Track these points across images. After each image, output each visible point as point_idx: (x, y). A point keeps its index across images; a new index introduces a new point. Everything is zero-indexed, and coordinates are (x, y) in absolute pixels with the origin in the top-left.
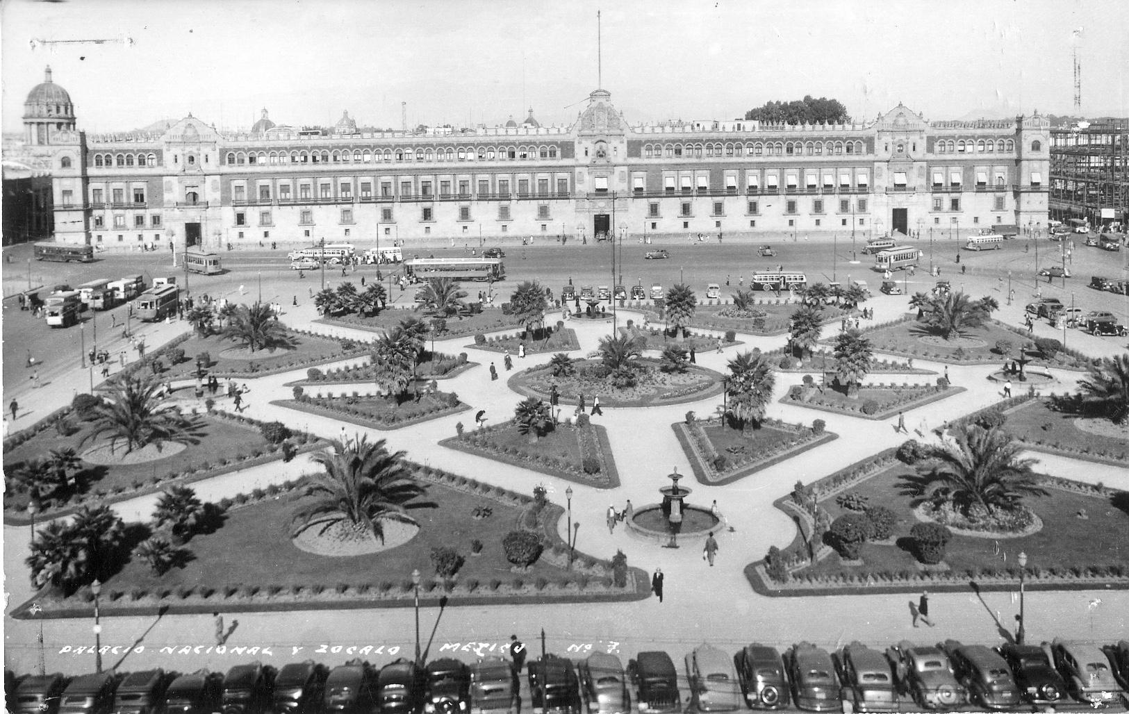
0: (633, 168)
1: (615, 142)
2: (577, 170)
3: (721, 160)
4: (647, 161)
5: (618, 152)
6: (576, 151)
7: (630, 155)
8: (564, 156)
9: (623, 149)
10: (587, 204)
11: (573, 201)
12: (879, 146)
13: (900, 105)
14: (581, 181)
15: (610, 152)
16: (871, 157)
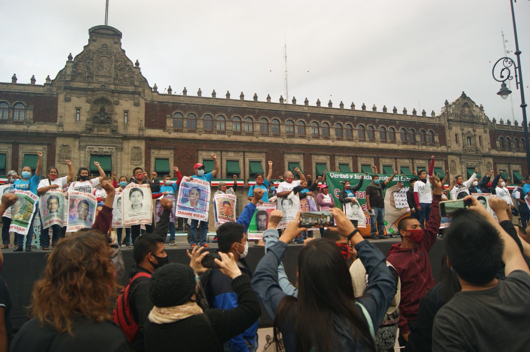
0: (152, 143)
1: (126, 104)
2: (60, 142)
3: (280, 140)
6: (60, 110)
7: (150, 124)
8: (38, 118)
9: (138, 114)
12: (450, 135)
13: (464, 96)
15: (119, 118)
16: (443, 149)
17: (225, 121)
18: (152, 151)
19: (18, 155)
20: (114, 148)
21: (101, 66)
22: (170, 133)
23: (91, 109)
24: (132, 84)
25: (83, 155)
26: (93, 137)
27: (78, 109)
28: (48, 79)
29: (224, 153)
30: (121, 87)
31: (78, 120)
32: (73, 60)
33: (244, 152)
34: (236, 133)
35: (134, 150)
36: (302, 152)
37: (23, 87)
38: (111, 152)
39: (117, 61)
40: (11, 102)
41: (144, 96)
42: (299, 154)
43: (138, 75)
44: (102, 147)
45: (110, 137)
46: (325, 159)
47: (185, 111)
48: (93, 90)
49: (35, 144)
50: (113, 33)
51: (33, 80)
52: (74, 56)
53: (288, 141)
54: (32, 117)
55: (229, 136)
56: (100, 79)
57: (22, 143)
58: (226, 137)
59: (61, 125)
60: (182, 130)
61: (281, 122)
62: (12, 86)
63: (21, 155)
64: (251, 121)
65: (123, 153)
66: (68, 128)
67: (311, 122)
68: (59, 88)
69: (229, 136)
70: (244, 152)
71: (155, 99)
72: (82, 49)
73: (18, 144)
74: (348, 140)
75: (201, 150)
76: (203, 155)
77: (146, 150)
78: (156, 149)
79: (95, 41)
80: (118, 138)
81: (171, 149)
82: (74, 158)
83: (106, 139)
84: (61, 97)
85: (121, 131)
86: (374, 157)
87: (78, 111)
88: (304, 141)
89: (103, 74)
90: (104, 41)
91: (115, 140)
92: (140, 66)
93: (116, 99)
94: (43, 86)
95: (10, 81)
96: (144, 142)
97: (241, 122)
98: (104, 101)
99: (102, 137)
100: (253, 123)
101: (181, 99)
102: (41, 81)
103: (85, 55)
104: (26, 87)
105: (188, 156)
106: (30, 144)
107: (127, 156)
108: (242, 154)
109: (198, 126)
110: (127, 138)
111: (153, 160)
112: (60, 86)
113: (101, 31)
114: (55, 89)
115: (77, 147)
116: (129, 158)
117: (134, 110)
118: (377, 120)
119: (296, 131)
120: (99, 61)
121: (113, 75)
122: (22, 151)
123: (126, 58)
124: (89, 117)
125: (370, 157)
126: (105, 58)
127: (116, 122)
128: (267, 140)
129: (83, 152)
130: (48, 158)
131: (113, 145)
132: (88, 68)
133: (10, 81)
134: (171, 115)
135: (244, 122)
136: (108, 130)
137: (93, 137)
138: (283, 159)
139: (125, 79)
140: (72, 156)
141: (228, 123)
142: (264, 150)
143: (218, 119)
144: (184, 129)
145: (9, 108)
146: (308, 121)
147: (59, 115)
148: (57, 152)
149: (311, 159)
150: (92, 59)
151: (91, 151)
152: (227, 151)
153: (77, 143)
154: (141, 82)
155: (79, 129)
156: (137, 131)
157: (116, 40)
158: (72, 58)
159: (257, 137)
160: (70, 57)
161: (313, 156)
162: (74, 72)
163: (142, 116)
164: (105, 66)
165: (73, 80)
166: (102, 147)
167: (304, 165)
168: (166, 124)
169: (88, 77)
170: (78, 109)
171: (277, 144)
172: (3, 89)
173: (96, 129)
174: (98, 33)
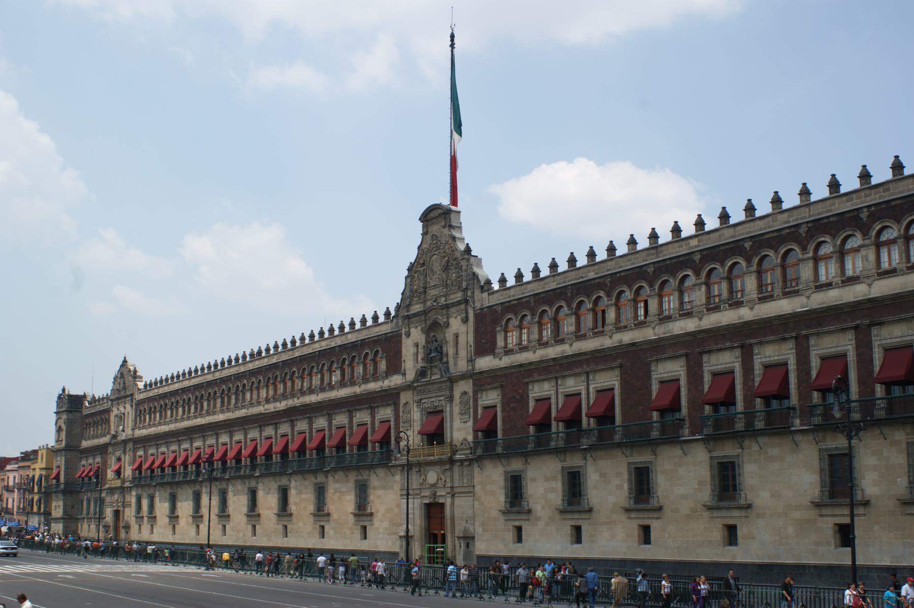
0: (482, 381)
20: (442, 398)
46: (733, 359)
55: (571, 345)
59: (404, 374)
69: (571, 345)
70: (587, 373)
74: (786, 294)
86: (856, 328)
88: (690, 325)
96: (471, 381)
108: (584, 378)
111: (480, 411)
113: (434, 214)
117: (463, 328)
118: (864, 215)
125: (843, 330)
142: (617, 363)
149: (700, 365)
167: (689, 382)
170: (417, 345)
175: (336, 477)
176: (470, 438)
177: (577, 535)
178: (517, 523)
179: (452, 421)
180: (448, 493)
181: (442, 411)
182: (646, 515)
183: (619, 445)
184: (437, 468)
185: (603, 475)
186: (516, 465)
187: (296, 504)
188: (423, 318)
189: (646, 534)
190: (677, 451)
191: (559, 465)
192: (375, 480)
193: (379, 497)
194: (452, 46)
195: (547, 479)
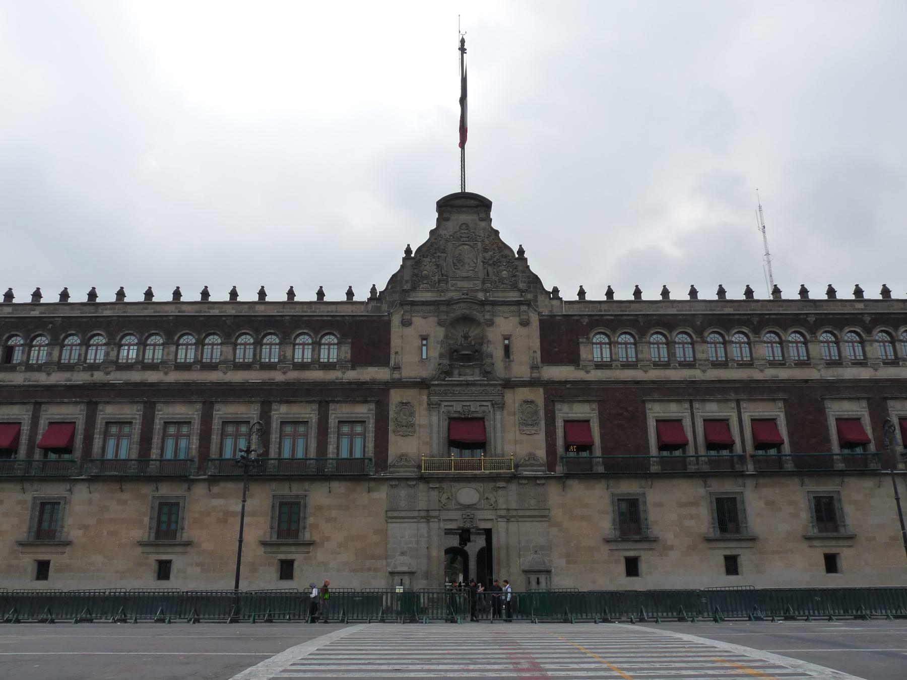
0: (557, 392)
1: (506, 323)
2: (396, 396)
3: (812, 374)
4: (595, 375)
5: (514, 340)
6: (395, 342)
7: (550, 356)
9: (528, 341)
10: (424, 497)
11: (381, 494)
14: (408, 428)
17: (692, 344)
18: (558, 406)
19: (327, 423)
20: (489, 404)
21: (459, 261)
22: (588, 372)
23: (446, 337)
24: (514, 287)
25: (435, 419)
26: (452, 385)
27: (424, 338)
28: (373, 290)
29: (696, 405)
30: (495, 294)
31: (424, 357)
32: (413, 255)
33: (738, 402)
34: (716, 365)
35: (525, 406)
36: (863, 395)
37: (334, 307)
38: (484, 412)
39: (486, 250)
40: (316, 333)
41: (537, 306)
42: (858, 399)
43: (523, 272)
44: (468, 404)
45: (481, 385)
47: (614, 330)
48: (448, 303)
49: (354, 402)
50: (476, 203)
51: (350, 294)
52: (414, 249)
53: (829, 374)
54: (349, 356)
55: (704, 371)
56: (460, 284)
57: (334, 402)
58: (697, 374)
59: (397, 368)
60: (611, 365)
61: (808, 337)
62: (318, 306)
63: (332, 421)
64: (746, 340)
65: (505, 412)
66: (411, 371)
67: (875, 332)
68: (391, 304)
69: (704, 371)
70: (738, 402)
71: (557, 312)
72: (426, 237)
73: (328, 403)
75: (650, 401)
76: (656, 411)
77: (546, 406)
78: (563, 402)
79: (447, 220)
80: (495, 385)
81: (594, 401)
82: (419, 426)
83: (474, 389)
84: (396, 320)
85: (500, 370)
87: (424, 342)
88: (865, 374)
89: (465, 275)
90: (464, 218)
91: (490, 389)
92: (525, 255)
93: (487, 317)
94: (367, 303)
95: (314, 298)
96: (541, 390)
97: (725, 343)
98: (467, 320)
99: (468, 384)
100: (749, 343)
101: (604, 307)
102: (362, 295)
103: (432, 245)
104: (339, 306)
105: (625, 414)
106: (346, 402)
107: (512, 418)
108: (733, 405)
109: (640, 356)
110: (509, 384)
111: (560, 424)
112: (394, 301)
114: (385, 307)
115: (425, 405)
116: (517, 422)
119: (843, 354)
120: (457, 252)
121: (481, 275)
122: (333, 416)
123: (500, 244)
124: (443, 351)
126: (466, 247)
127: (491, 356)
128: (783, 374)
129: (435, 413)
130: (375, 427)
131: (487, 398)
132: (438, 266)
133: (314, 298)
134: (588, 338)
135: (733, 342)
136: (477, 371)
137: (452, 385)
138: (821, 412)
139: (501, 281)
140: (417, 422)
141: (698, 347)
142: (781, 395)
143: (677, 340)
144: (614, 364)
145: (312, 344)
146: (869, 331)
147: (393, 351)
148: (392, 415)
149: (885, 410)
150: (444, 251)
151: (449, 412)
152: (703, 401)
153: (425, 397)
154: (529, 283)
155: (425, 372)
156: (529, 370)
157: (483, 215)
158: (411, 252)
159: (762, 371)
160: (408, 251)
161: (890, 403)
162: (417, 275)
163: (536, 343)
164: (467, 261)
165: (414, 288)
166: (468, 404)
167: (873, 422)
168: (579, 355)
169: (439, 281)
171: (806, 381)
172: (303, 312)
173: (456, 372)
174: (452, 206)
175: (215, 489)
176: (541, 453)
177: (732, 565)
178: (632, 554)
179: (495, 433)
180: (501, 517)
181: (482, 419)
182: (833, 543)
183: (790, 474)
184: (479, 486)
185: (770, 503)
186: (628, 487)
187: (86, 527)
188: (443, 308)
189: (831, 563)
190: (868, 483)
191: (702, 491)
192: (319, 496)
193: (329, 520)
194: (463, 50)
195: (681, 505)
